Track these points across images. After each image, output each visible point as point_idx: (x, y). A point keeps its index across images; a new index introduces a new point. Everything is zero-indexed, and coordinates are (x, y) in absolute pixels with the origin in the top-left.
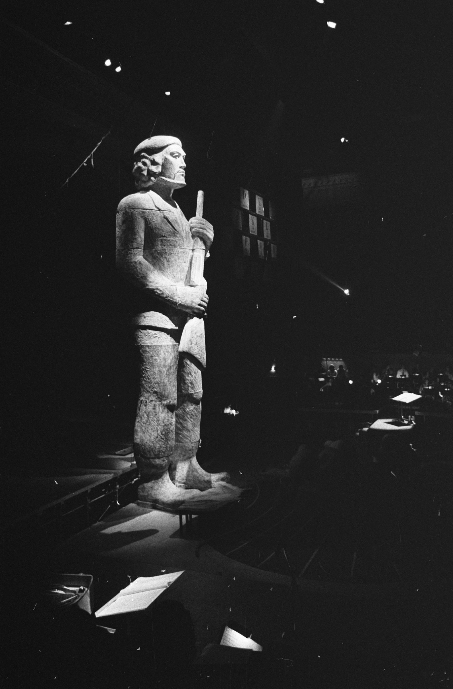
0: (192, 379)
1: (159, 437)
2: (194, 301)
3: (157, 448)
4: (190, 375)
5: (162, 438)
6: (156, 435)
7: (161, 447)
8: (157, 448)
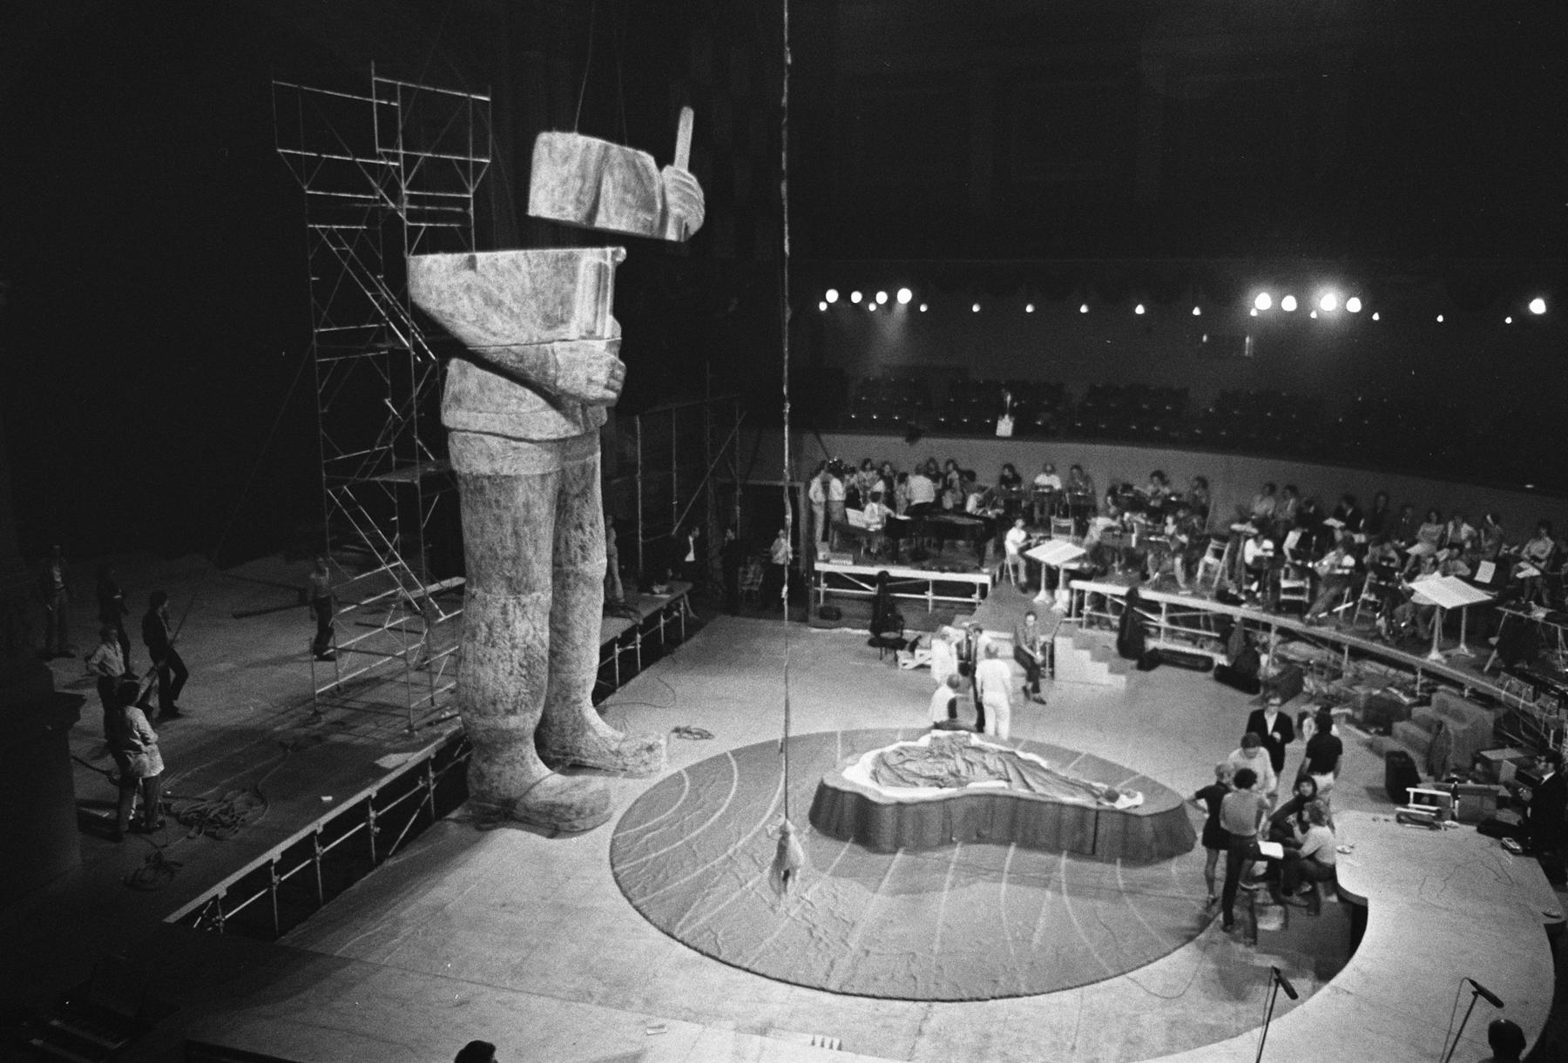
0: (585, 538)
6: (508, 668)
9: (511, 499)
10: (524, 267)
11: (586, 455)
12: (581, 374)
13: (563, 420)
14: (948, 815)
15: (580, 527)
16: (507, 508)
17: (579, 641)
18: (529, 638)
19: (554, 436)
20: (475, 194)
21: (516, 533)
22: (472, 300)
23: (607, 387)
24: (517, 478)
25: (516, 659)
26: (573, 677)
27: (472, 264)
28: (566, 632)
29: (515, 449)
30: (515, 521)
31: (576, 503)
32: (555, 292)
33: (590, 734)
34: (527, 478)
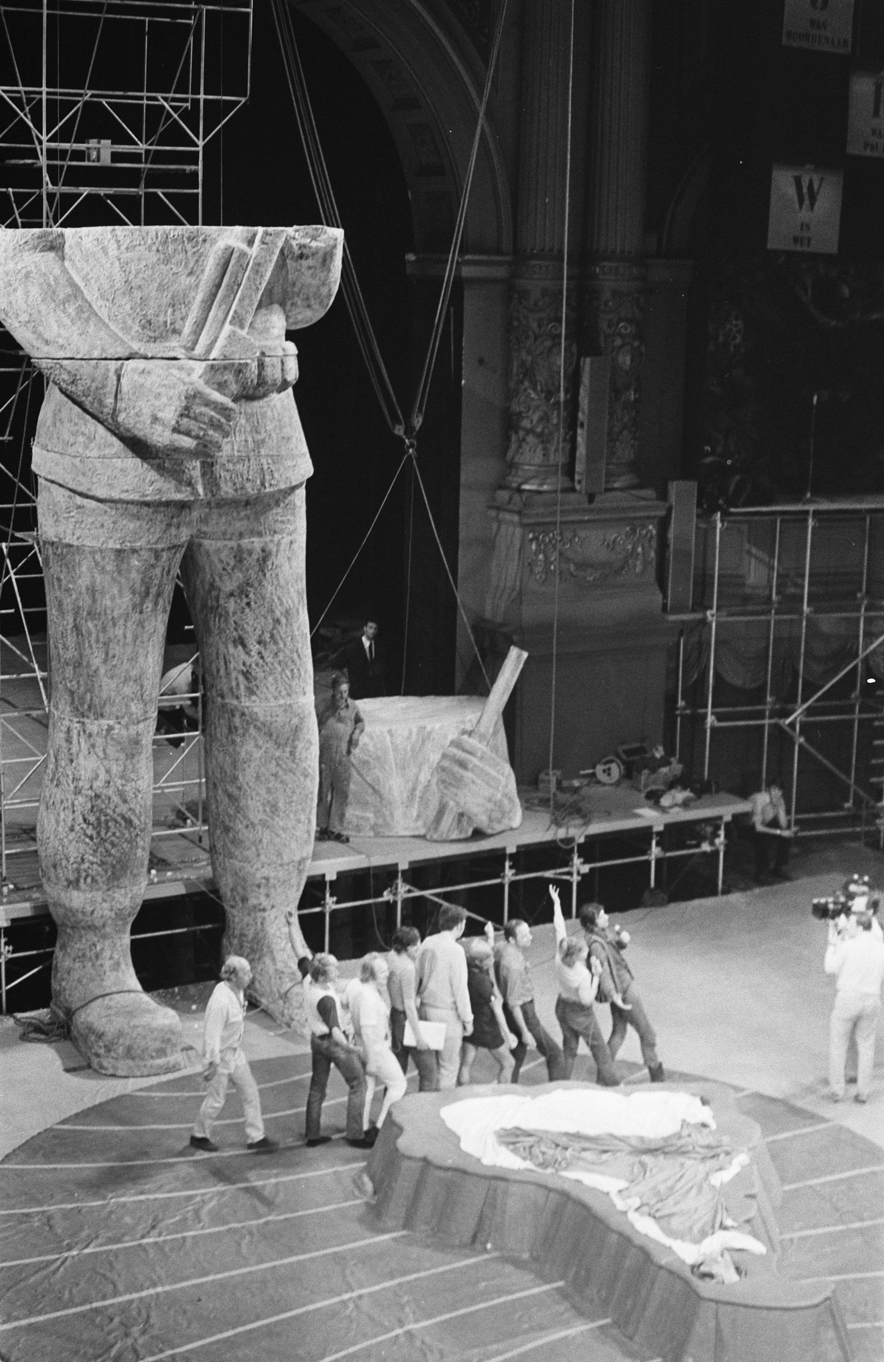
0: (248, 661)
1: (77, 828)
2: (160, 415)
3: (72, 860)
4: (240, 648)
5: (86, 835)
7: (83, 860)
8: (72, 860)
9: (75, 583)
10: (113, 251)
11: (241, 535)
12: (145, 408)
13: (152, 475)
14: (491, 1202)
15: (241, 642)
16: (68, 590)
18: (98, 784)
19: (135, 497)
20: (204, 147)
21: (77, 628)
22: (27, 293)
23: (176, 430)
27: (56, 247)
28: (236, 800)
29: (79, 507)
31: (231, 605)
32: (161, 288)
33: (267, 960)
34: (93, 553)
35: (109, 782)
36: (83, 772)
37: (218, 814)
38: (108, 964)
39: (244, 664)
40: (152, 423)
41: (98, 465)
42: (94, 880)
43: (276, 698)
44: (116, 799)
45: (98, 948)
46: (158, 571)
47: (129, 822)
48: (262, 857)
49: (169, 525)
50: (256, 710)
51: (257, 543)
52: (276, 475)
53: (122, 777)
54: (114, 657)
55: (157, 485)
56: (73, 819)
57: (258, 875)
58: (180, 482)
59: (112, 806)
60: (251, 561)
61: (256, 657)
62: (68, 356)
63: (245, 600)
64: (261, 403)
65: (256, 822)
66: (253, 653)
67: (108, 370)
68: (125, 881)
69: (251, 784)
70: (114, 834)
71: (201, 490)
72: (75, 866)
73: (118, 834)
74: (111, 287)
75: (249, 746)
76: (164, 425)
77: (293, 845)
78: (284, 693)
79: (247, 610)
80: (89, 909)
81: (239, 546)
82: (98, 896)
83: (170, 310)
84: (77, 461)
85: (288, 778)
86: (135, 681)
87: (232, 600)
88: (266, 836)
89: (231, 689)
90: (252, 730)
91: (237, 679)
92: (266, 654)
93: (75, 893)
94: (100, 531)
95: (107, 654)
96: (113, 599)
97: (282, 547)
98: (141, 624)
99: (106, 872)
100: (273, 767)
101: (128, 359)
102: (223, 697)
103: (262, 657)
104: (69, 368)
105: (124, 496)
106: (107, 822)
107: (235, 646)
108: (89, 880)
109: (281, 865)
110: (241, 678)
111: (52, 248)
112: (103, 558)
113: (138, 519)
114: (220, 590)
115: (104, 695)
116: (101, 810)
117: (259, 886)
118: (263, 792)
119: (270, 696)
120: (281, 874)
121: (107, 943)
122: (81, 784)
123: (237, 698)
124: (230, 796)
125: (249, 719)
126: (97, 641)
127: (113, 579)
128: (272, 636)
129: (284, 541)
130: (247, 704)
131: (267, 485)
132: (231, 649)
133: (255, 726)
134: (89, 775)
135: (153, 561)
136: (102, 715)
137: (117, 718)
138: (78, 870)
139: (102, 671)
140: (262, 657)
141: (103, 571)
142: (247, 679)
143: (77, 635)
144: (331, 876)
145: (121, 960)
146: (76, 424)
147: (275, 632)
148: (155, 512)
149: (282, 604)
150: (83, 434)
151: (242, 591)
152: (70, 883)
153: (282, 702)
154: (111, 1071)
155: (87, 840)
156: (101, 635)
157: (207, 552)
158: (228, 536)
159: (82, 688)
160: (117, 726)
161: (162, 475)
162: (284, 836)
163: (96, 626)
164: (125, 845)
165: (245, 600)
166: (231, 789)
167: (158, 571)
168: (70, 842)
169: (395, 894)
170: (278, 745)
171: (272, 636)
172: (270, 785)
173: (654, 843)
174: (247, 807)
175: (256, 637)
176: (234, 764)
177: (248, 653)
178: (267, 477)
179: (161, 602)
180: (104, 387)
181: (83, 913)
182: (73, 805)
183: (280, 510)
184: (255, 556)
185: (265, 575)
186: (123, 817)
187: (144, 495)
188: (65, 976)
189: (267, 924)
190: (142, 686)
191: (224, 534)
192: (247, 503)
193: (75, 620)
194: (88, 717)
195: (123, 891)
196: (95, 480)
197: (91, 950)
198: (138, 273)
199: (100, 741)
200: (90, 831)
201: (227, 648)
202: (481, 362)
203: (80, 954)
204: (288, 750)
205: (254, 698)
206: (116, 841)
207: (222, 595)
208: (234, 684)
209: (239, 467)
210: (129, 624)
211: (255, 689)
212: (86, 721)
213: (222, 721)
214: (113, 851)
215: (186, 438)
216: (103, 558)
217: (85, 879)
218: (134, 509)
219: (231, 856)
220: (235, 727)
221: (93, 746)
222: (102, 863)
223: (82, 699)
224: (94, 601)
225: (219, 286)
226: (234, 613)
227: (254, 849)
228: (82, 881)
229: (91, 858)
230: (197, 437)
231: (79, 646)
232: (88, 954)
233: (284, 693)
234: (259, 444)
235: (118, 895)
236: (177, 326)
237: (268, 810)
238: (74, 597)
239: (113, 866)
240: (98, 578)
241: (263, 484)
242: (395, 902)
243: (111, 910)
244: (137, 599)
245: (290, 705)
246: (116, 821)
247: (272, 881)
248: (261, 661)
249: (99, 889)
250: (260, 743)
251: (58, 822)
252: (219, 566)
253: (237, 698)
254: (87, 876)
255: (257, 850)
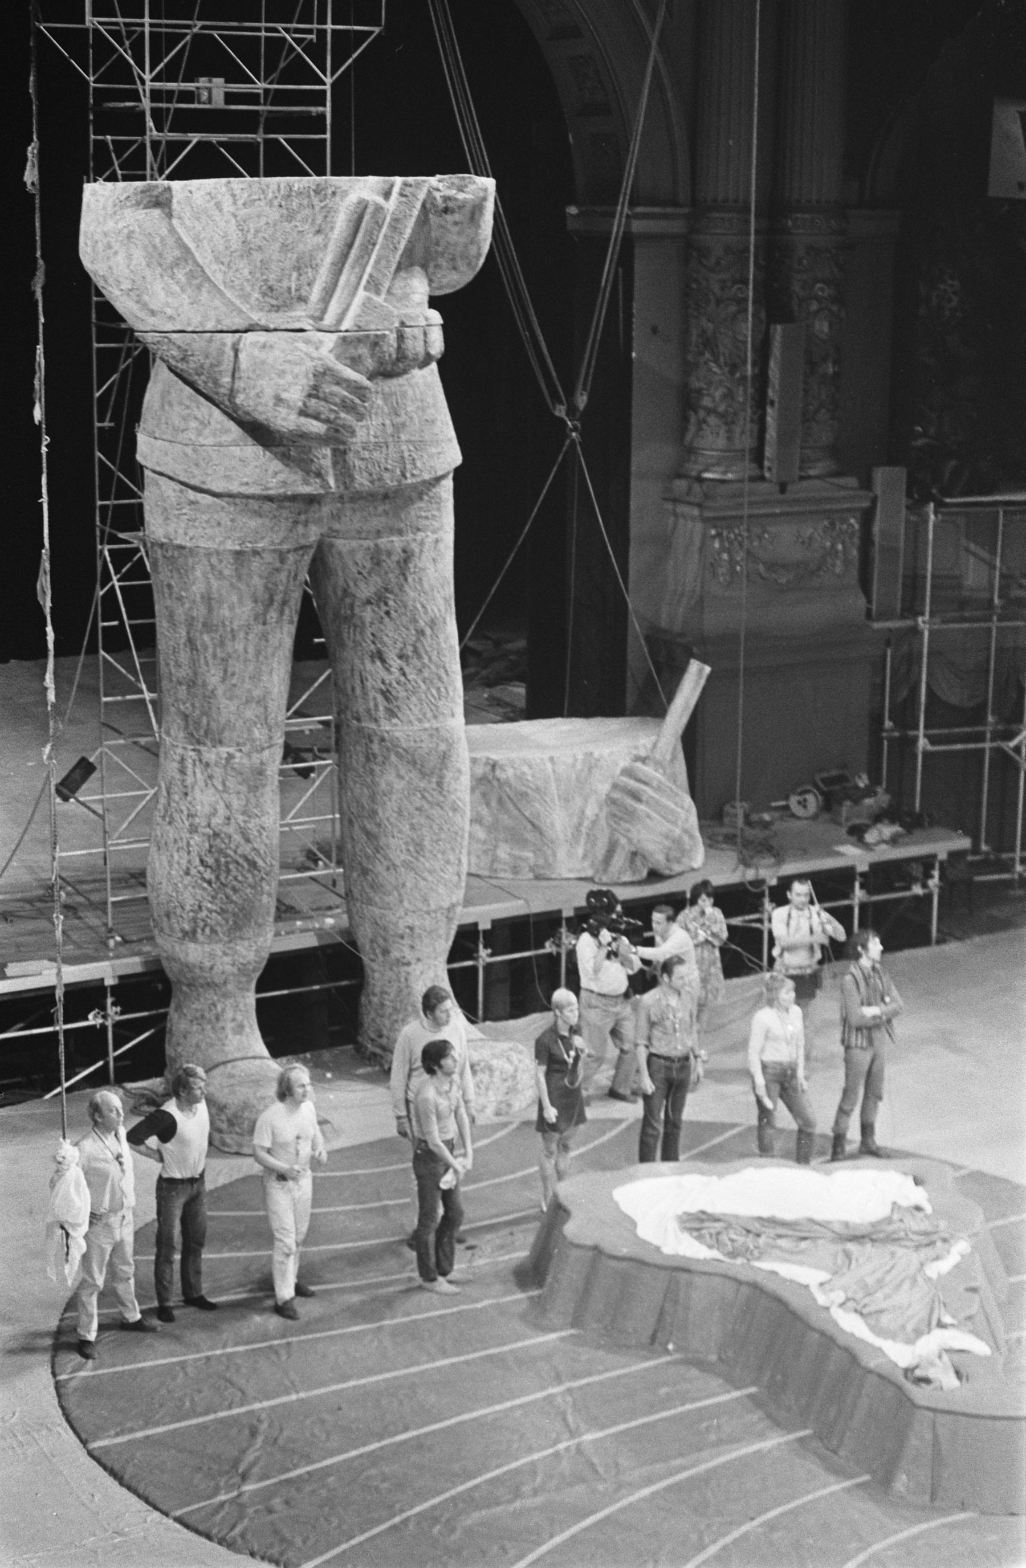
0: (388, 678)
1: (193, 871)
2: (284, 395)
3: (188, 908)
4: (378, 663)
5: (203, 879)
7: (200, 907)
9: (186, 590)
10: (227, 206)
11: (379, 534)
12: (268, 387)
13: (276, 465)
15: (380, 656)
16: (180, 599)
17: (399, 856)
18: (217, 821)
20: (333, 85)
21: (191, 641)
22: (129, 257)
23: (303, 413)
24: (192, 551)
25: (195, 850)
26: (391, 917)
27: (162, 203)
28: (376, 838)
29: (192, 503)
30: (190, 622)
31: (368, 614)
32: (285, 248)
34: (208, 555)
35: (229, 819)
36: (199, 808)
37: (355, 854)
38: (230, 1025)
39: (383, 682)
40: (275, 405)
41: (214, 455)
42: (213, 931)
43: (420, 721)
44: (237, 838)
45: (219, 1008)
46: (283, 576)
47: (253, 864)
48: (406, 904)
49: (296, 523)
50: (397, 734)
51: (397, 542)
52: (419, 464)
53: (244, 813)
54: (233, 674)
55: (281, 477)
56: (189, 862)
57: (402, 924)
58: (308, 472)
59: (232, 846)
60: (390, 563)
61: (397, 673)
62: (179, 328)
63: (384, 608)
64: (401, 380)
65: (398, 862)
66: (393, 670)
67: (224, 344)
68: (248, 932)
69: (392, 820)
70: (235, 878)
71: (332, 482)
72: (191, 914)
73: (240, 878)
74: (227, 248)
75: (391, 776)
76: (289, 407)
77: (441, 890)
78: (429, 715)
79: (387, 620)
80: (208, 964)
81: (376, 545)
82: (218, 948)
83: (295, 275)
84: (189, 450)
85: (435, 812)
86: (258, 702)
87: (369, 608)
88: (410, 879)
89: (368, 711)
90: (393, 758)
91: (375, 699)
92: (407, 670)
93: (192, 945)
94: (217, 529)
95: (225, 671)
96: (232, 608)
97: (427, 547)
98: (264, 637)
99: (227, 921)
100: (417, 801)
101: (246, 331)
102: (359, 720)
103: (404, 674)
104: (179, 343)
105: (243, 490)
106: (227, 863)
107: (373, 662)
108: (207, 930)
109: (428, 913)
110: (380, 698)
111: (157, 204)
112: (221, 561)
113: (261, 516)
114: (354, 596)
115: (223, 721)
116: (221, 851)
117: (402, 937)
118: (406, 828)
119: (412, 718)
120: (427, 923)
121: (228, 1002)
122: (197, 820)
123: (376, 720)
124: (368, 833)
125: (389, 745)
126: (214, 656)
127: (232, 585)
128: (416, 651)
129: (429, 540)
130: (388, 728)
131: (408, 475)
132: (369, 666)
133: (397, 754)
134: (207, 810)
135: (278, 565)
136: (221, 742)
137: (238, 744)
138: (194, 920)
139: (220, 692)
140: (404, 674)
141: (220, 575)
142: (387, 699)
143: (192, 650)
144: (485, 925)
145: (246, 1023)
146: (188, 407)
147: (418, 645)
148: (281, 507)
149: (426, 612)
150: (196, 418)
151: (380, 599)
152: (185, 933)
153: (427, 725)
154: (235, 1149)
155: (205, 885)
156: (218, 650)
157: (340, 553)
158: (363, 535)
159: (198, 712)
160: (238, 754)
161: (287, 465)
162: (430, 878)
163: (212, 639)
164: (248, 891)
165: (384, 608)
166: (370, 826)
167: (283, 576)
168: (186, 887)
169: (558, 946)
170: (423, 775)
171: (416, 651)
172: (414, 821)
173: (857, 885)
174: (388, 846)
175: (397, 651)
176: (373, 798)
177: (388, 670)
178: (409, 466)
179: (287, 611)
180: (219, 363)
181: (201, 968)
182: (188, 845)
183: (422, 504)
184: (395, 558)
185: (406, 580)
186: (246, 859)
187: (267, 489)
188: (182, 1040)
189: (412, 978)
190: (266, 708)
191: (359, 532)
192: (386, 496)
193: (188, 633)
194: (204, 744)
195: (246, 943)
196: (210, 472)
197: (210, 1010)
198: (257, 231)
199: (218, 772)
200: (208, 875)
201: (363, 664)
202: (655, 330)
203: (198, 1015)
204: (434, 780)
205: (395, 721)
206: (238, 886)
207: (358, 603)
208: (372, 704)
209: (376, 455)
210: (250, 637)
211: (396, 710)
212: (202, 748)
213: (358, 748)
214: (234, 898)
215: (315, 422)
216: (221, 561)
217: (203, 930)
218: (254, 505)
219: (370, 902)
220: (375, 756)
221: (211, 777)
222: (222, 912)
223: (197, 724)
224: (210, 610)
225: (350, 246)
226: (372, 623)
227: (396, 894)
228: (199, 931)
229: (209, 905)
230: (327, 421)
231: (194, 663)
232: (207, 1015)
233: (429, 715)
234: (399, 428)
235: (241, 947)
236: (304, 293)
237: (411, 848)
238: (187, 605)
239: (235, 915)
240: (215, 584)
241: (404, 475)
242: (559, 954)
243: (233, 965)
244: (260, 608)
245: (437, 729)
246: (237, 863)
247: (417, 931)
248: (403, 679)
249: (220, 941)
250: (403, 772)
251: (170, 864)
252: (354, 570)
253: (376, 720)
254: (206, 925)
255: (400, 895)
